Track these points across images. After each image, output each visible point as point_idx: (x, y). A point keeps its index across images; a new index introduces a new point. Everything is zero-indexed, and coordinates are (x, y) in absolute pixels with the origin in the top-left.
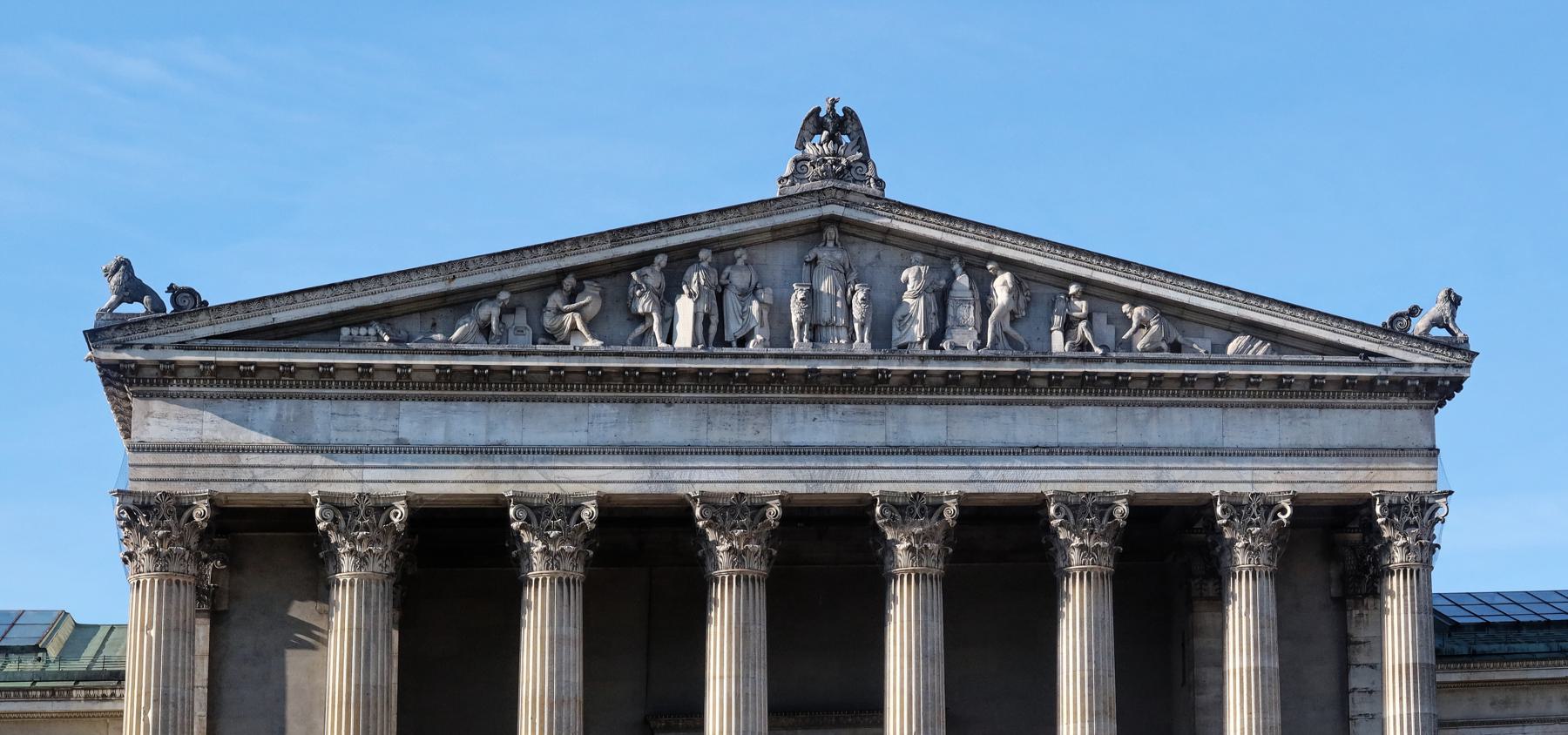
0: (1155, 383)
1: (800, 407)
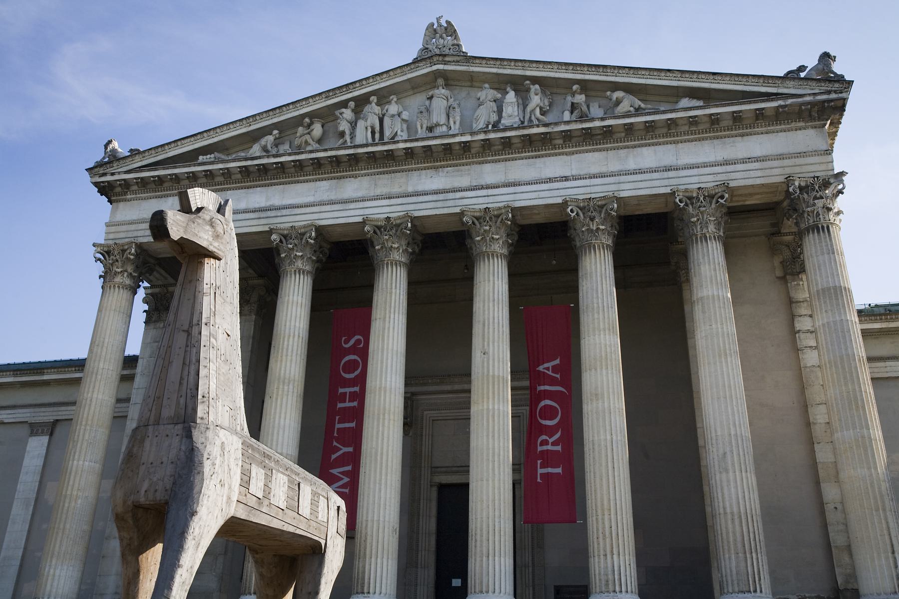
1: (424, 171)
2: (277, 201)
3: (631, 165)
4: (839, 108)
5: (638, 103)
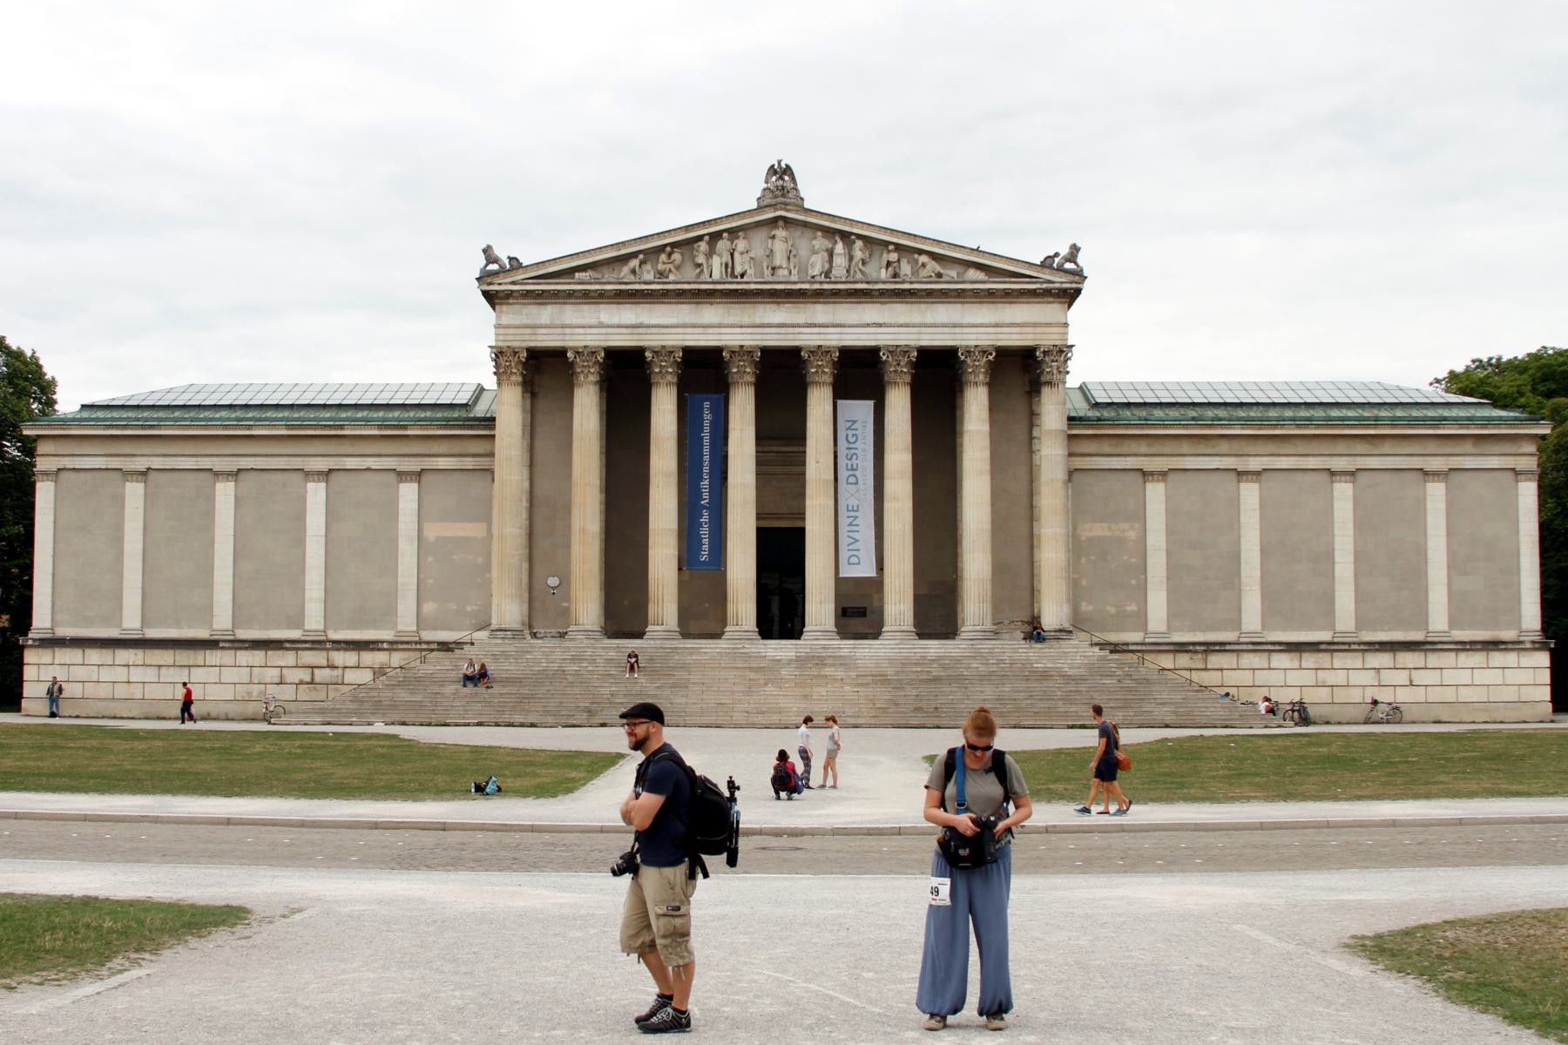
0: (930, 294)
2: (646, 320)
3: (929, 320)
4: (1078, 292)
5: (938, 268)
